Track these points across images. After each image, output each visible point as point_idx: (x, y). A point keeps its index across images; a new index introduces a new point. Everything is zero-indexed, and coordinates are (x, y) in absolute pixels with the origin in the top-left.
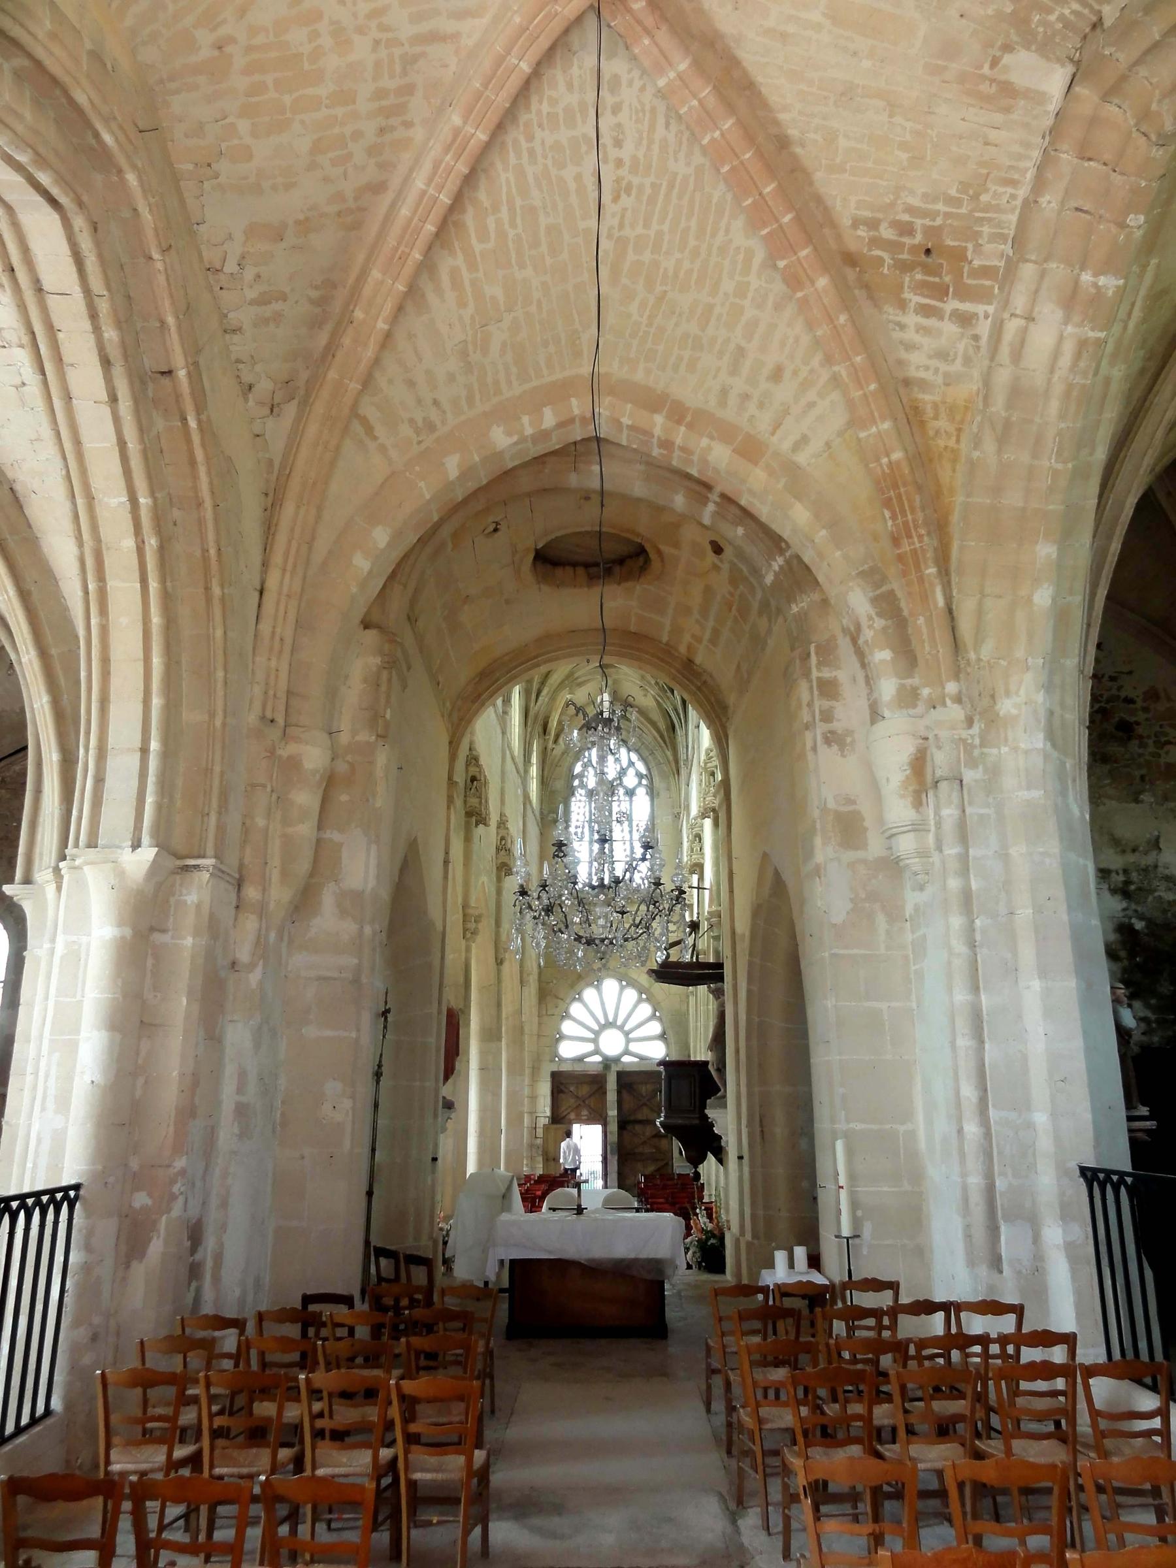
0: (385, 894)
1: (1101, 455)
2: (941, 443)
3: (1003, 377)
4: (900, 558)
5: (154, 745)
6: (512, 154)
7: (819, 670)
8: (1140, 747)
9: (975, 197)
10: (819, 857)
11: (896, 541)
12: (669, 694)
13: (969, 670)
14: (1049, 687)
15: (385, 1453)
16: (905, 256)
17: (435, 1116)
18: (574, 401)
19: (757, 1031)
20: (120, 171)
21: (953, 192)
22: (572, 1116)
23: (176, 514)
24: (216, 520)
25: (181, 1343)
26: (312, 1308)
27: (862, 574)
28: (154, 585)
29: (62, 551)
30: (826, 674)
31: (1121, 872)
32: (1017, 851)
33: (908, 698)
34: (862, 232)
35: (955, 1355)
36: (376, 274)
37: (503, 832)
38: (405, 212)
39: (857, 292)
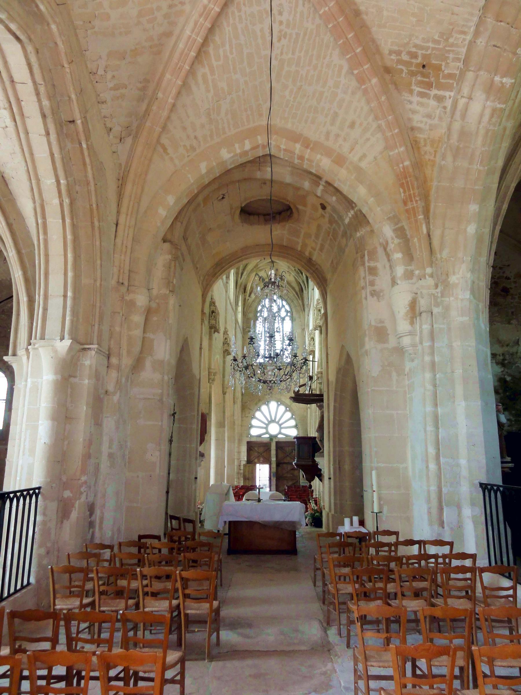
0: (173, 362)
1: (500, 163)
2: (427, 157)
3: (457, 126)
4: (407, 211)
5: (70, 294)
6: (231, 19)
7: (368, 262)
8: (511, 299)
9: (447, 40)
10: (367, 347)
11: (405, 203)
12: (301, 275)
13: (437, 262)
14: (472, 271)
15: (175, 602)
16: (413, 68)
17: (196, 459)
18: (259, 137)
19: (338, 424)
20: (48, 24)
21: (436, 37)
22: (256, 460)
23: (77, 188)
24: (96, 191)
25: (86, 555)
26: (142, 541)
27: (389, 219)
28: (68, 221)
29: (26, 206)
30: (372, 264)
31: (501, 355)
32: (457, 344)
33: (409, 275)
34: (393, 57)
35: (423, 563)
36: (168, 76)
37: (226, 336)
38: (181, 45)
39: (390, 86)
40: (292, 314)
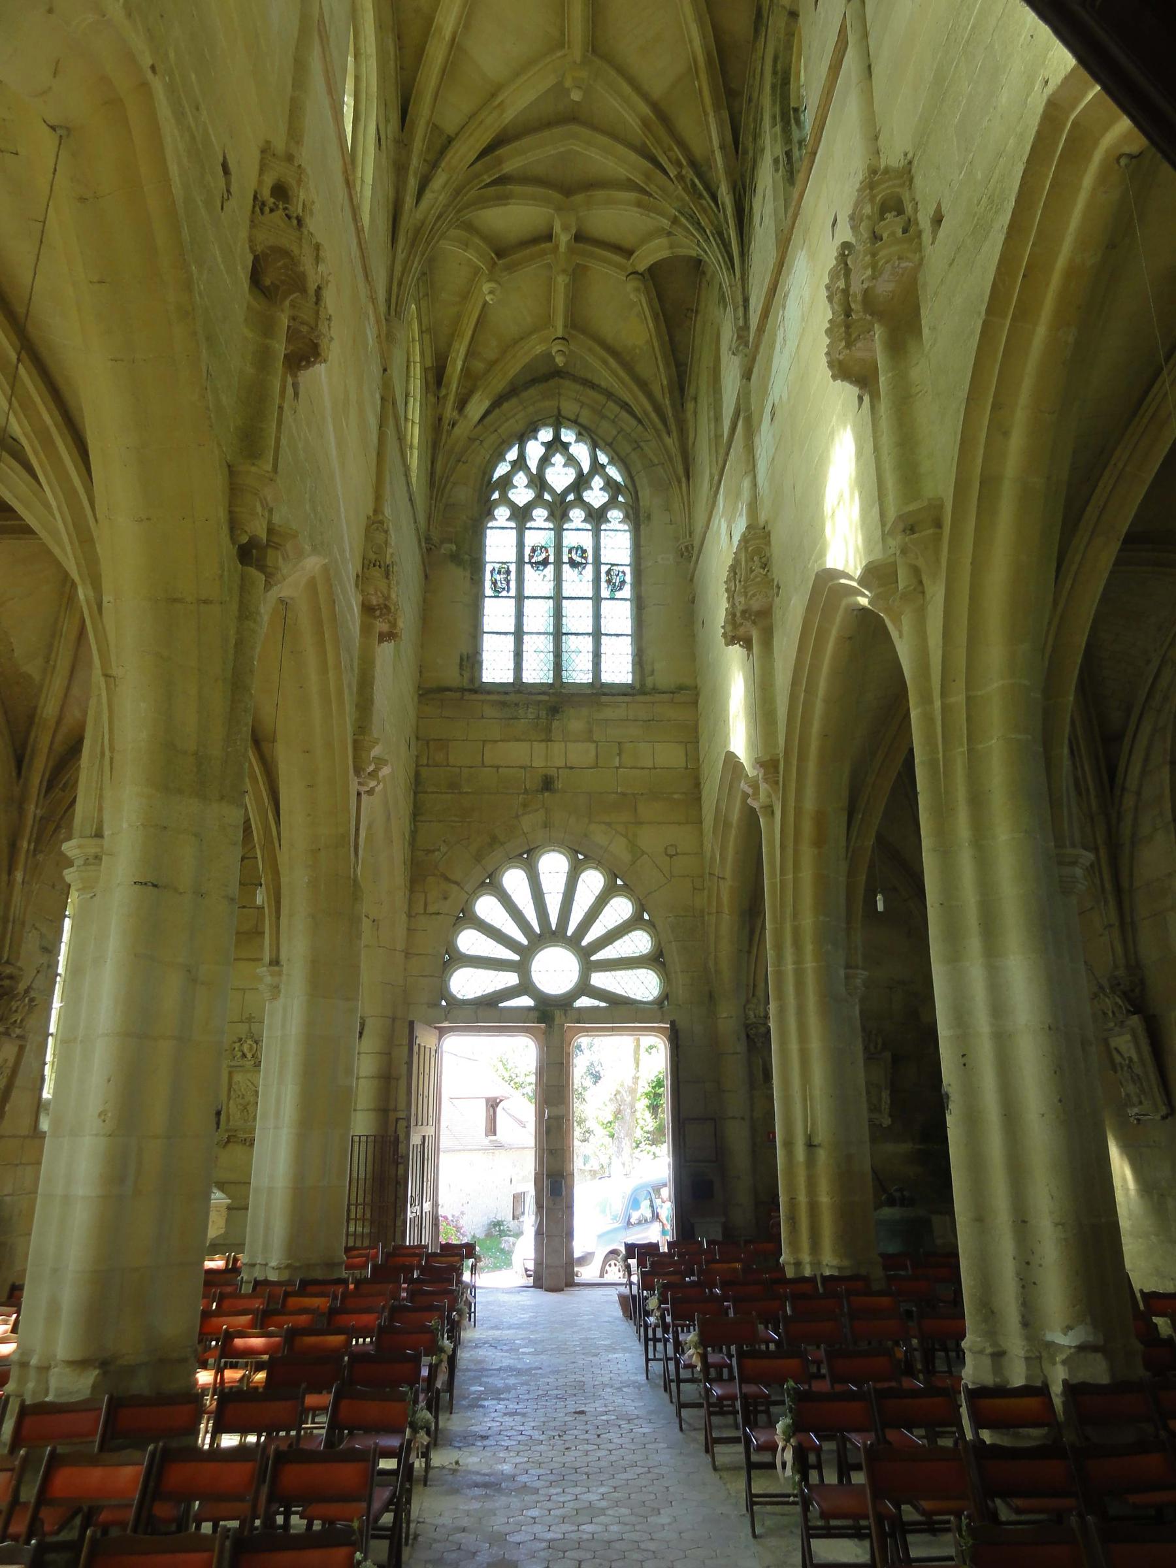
40: (635, 497)
